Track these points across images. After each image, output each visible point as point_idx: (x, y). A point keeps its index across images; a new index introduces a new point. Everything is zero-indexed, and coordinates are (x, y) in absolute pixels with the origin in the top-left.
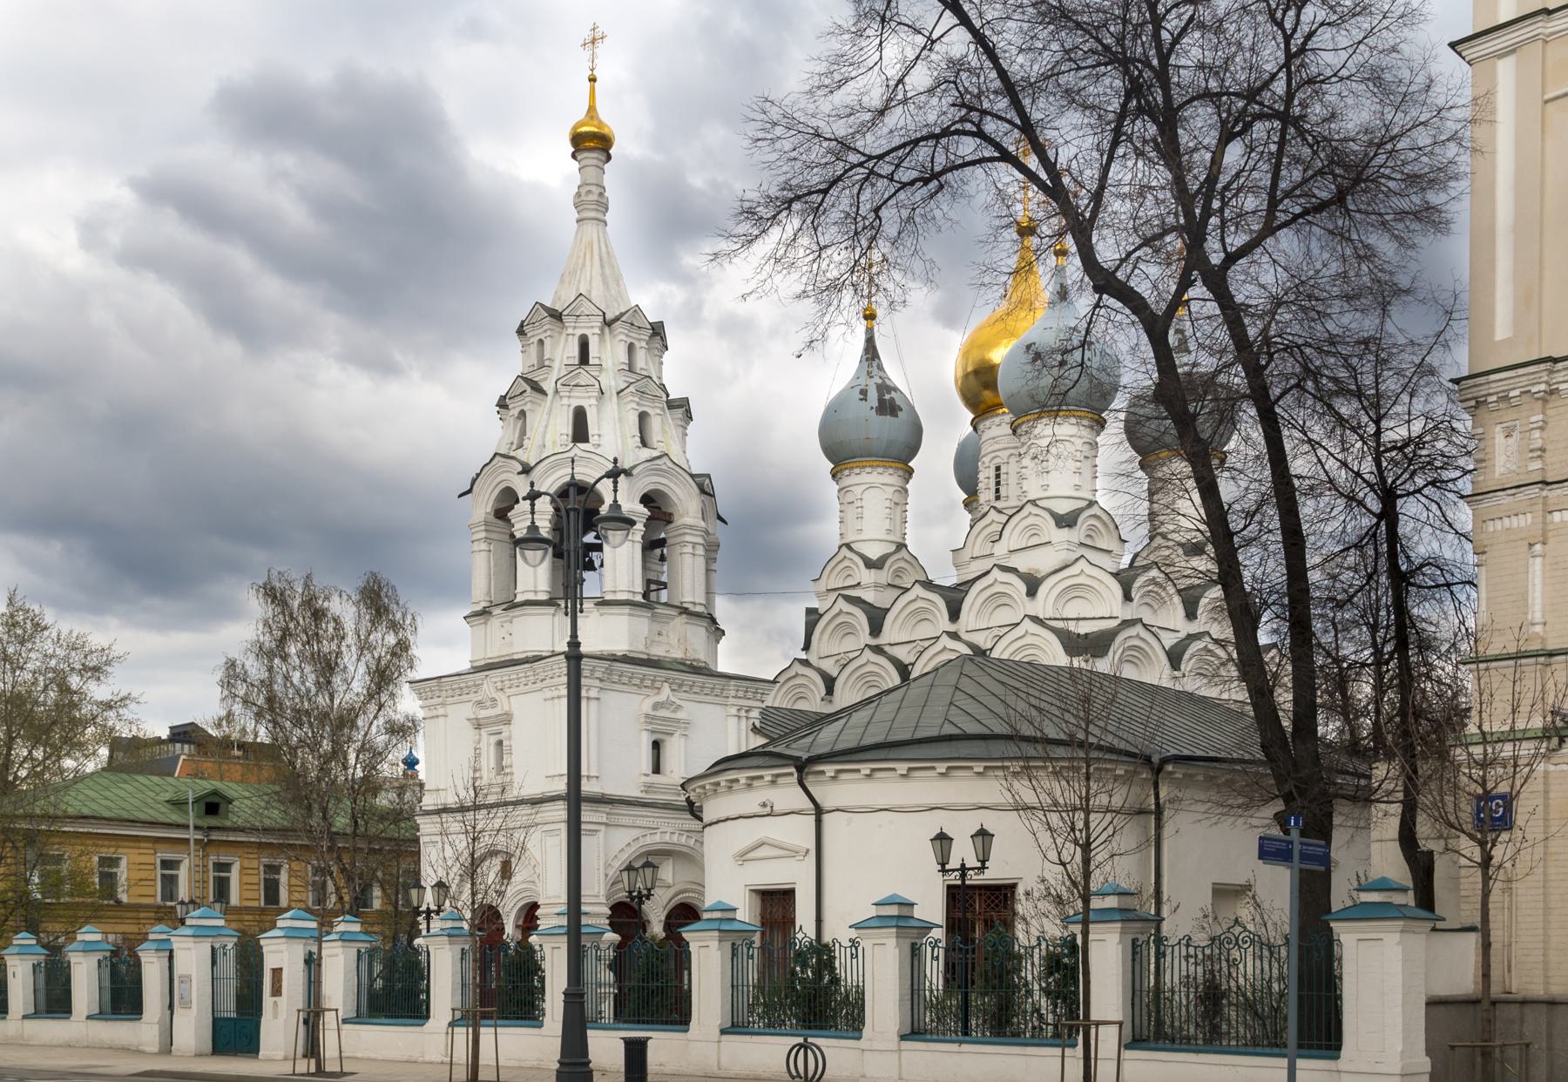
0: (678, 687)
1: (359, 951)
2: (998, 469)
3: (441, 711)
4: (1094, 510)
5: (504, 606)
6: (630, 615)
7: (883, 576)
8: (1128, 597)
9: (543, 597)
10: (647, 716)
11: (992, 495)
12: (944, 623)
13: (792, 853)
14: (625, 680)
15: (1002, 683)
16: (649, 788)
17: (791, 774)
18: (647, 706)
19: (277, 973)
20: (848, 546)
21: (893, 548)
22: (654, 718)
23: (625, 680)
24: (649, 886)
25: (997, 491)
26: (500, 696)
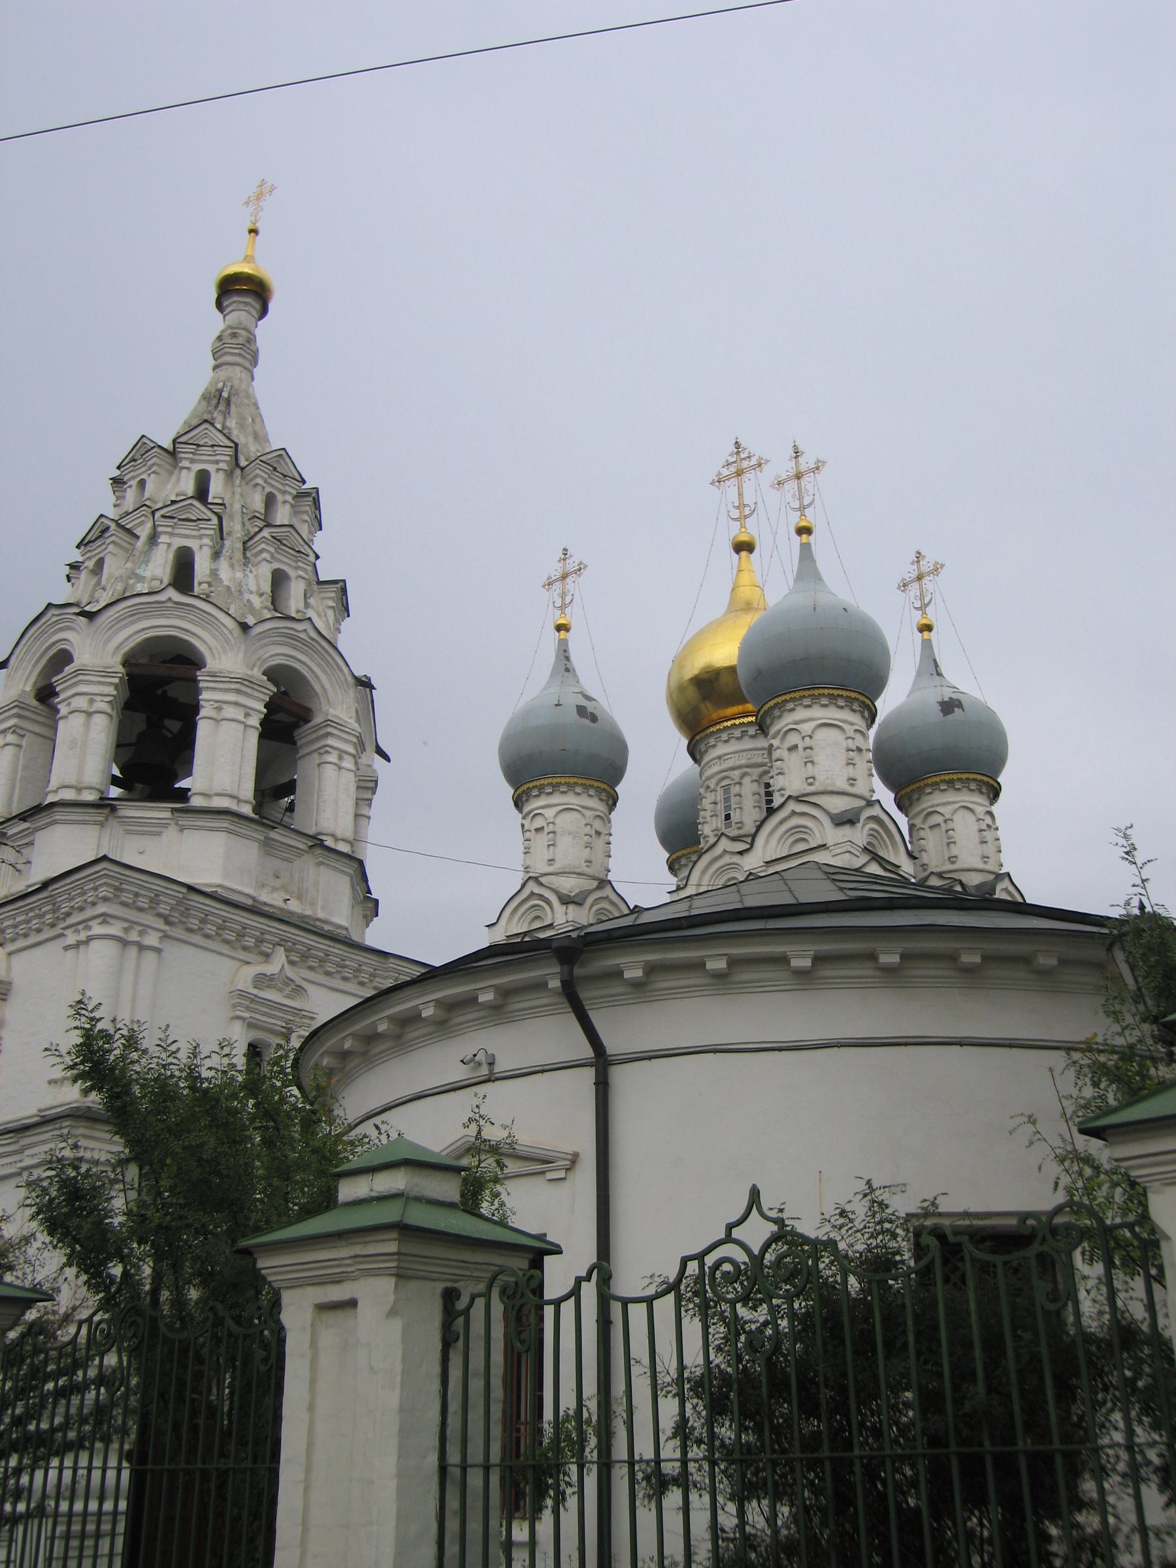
0: (303, 958)
2: (726, 789)
4: (876, 811)
6: (230, 832)
9: (90, 796)
10: (242, 994)
11: (719, 822)
14: (210, 929)
17: (539, 986)
18: (245, 977)
20: (536, 879)
21: (595, 884)
22: (254, 999)
23: (210, 929)
25: (728, 817)
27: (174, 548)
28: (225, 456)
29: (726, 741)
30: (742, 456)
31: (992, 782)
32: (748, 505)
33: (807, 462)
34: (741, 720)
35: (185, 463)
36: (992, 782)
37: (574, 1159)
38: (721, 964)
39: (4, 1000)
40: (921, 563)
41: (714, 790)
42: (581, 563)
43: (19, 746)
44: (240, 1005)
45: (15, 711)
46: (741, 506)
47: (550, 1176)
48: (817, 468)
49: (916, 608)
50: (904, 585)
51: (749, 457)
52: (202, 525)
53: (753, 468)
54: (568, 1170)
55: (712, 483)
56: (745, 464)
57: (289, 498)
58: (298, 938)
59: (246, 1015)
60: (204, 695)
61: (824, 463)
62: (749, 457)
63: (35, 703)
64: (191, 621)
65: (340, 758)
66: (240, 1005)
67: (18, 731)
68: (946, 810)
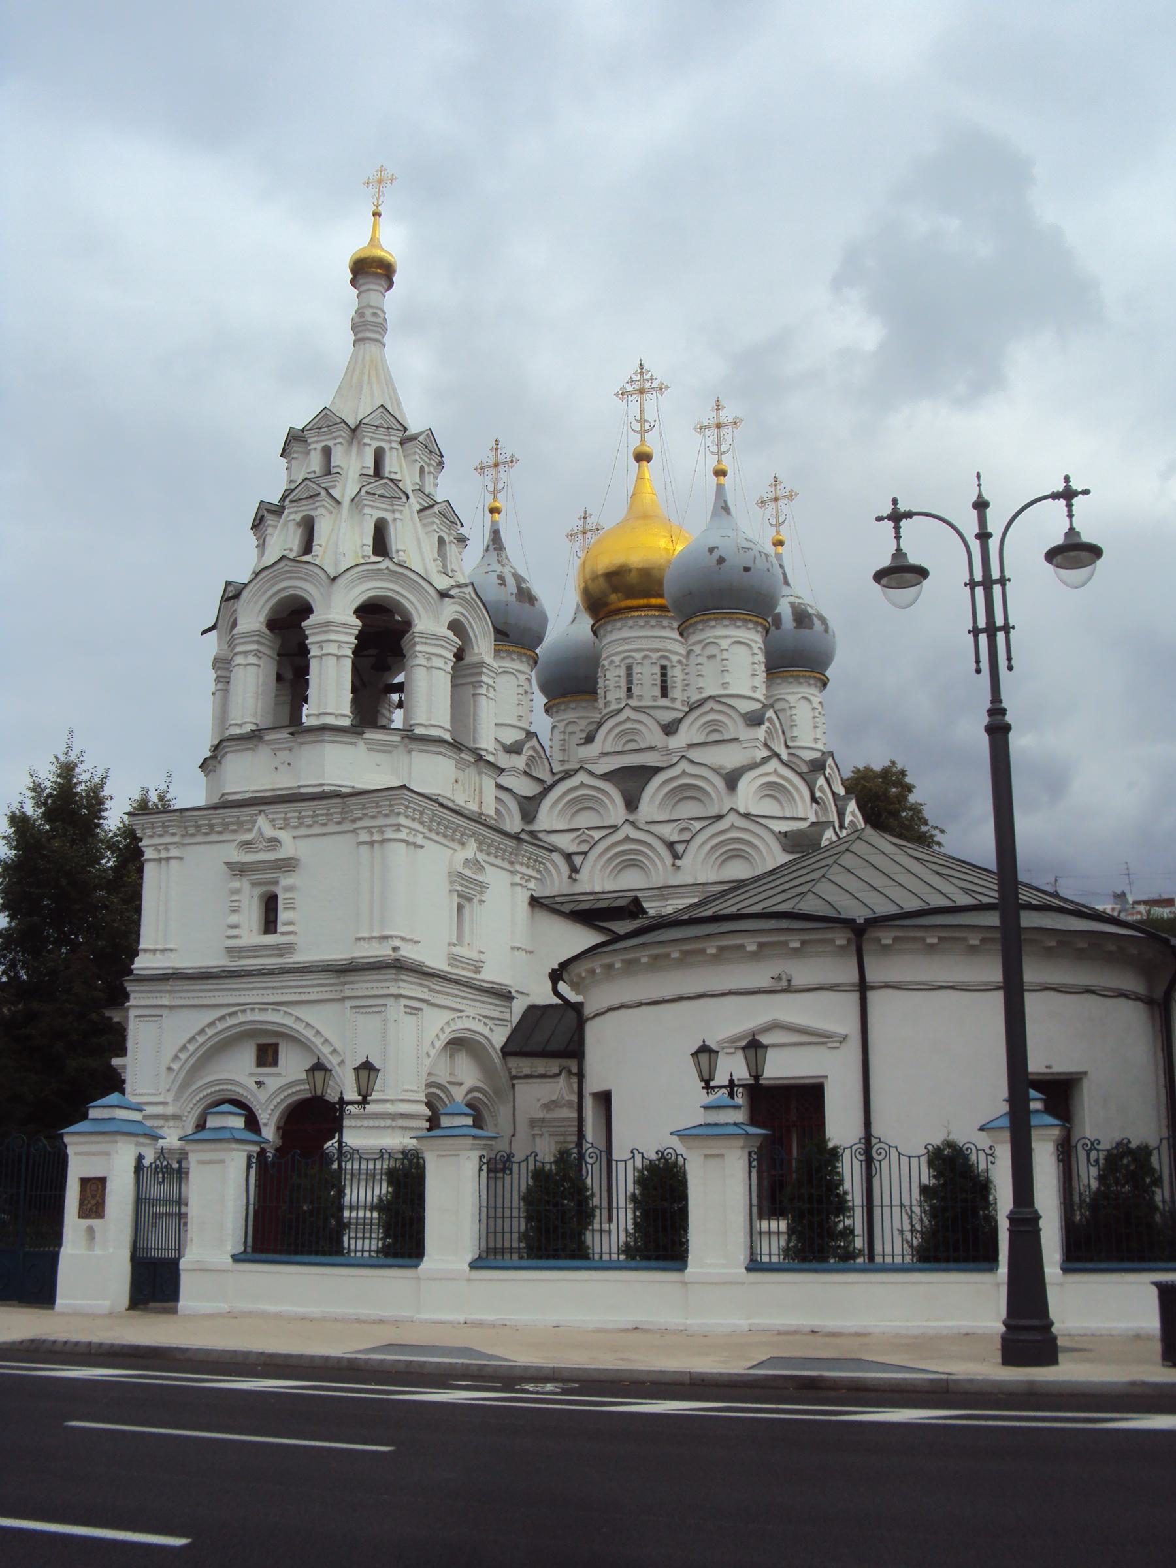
1: (249, 1157)
2: (629, 668)
3: (174, 852)
5: (291, 730)
7: (519, 762)
8: (814, 799)
9: (346, 722)
10: (460, 875)
11: (622, 693)
12: (616, 812)
13: (823, 1039)
15: (917, 859)
16: (454, 959)
19: (94, 1190)
21: (524, 735)
24: (706, 1077)
25: (629, 689)
26: (283, 836)
27: (375, 518)
28: (396, 437)
29: (631, 627)
30: (645, 377)
31: (822, 677)
32: (648, 421)
33: (727, 415)
34: (647, 613)
35: (366, 441)
36: (822, 677)
37: (845, 1038)
38: (935, 941)
39: (294, 871)
40: (779, 487)
41: (619, 666)
42: (512, 456)
43: (259, 666)
44: (456, 881)
45: (256, 638)
46: (642, 421)
47: (829, 1045)
48: (735, 423)
49: (771, 525)
50: (762, 502)
51: (652, 379)
52: (396, 502)
53: (654, 389)
54: (840, 1043)
55: (617, 394)
56: (648, 385)
57: (432, 469)
58: (481, 832)
59: (459, 888)
60: (419, 648)
61: (741, 421)
62: (652, 379)
63: (267, 632)
64: (402, 587)
65: (487, 689)
66: (456, 881)
67: (259, 654)
68: (791, 698)
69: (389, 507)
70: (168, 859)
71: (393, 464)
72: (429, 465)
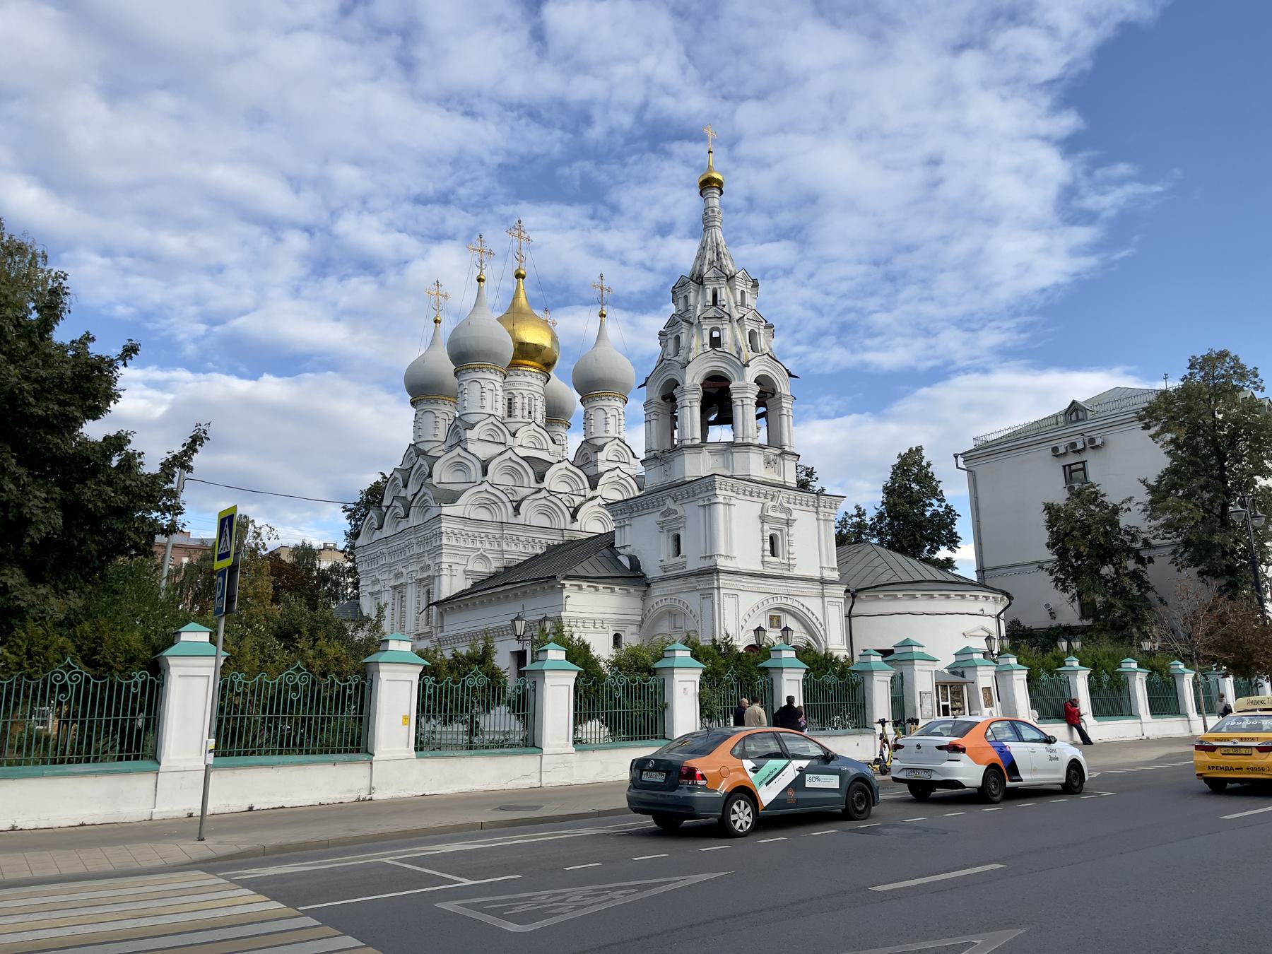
63: (662, 402)
69: (720, 323)
70: (624, 526)
71: (724, 294)
72: (747, 288)
